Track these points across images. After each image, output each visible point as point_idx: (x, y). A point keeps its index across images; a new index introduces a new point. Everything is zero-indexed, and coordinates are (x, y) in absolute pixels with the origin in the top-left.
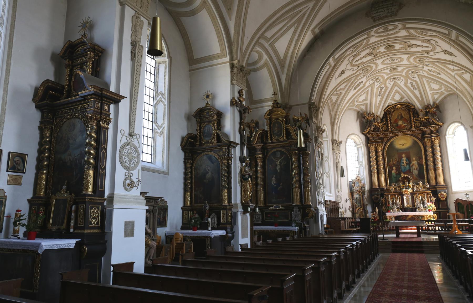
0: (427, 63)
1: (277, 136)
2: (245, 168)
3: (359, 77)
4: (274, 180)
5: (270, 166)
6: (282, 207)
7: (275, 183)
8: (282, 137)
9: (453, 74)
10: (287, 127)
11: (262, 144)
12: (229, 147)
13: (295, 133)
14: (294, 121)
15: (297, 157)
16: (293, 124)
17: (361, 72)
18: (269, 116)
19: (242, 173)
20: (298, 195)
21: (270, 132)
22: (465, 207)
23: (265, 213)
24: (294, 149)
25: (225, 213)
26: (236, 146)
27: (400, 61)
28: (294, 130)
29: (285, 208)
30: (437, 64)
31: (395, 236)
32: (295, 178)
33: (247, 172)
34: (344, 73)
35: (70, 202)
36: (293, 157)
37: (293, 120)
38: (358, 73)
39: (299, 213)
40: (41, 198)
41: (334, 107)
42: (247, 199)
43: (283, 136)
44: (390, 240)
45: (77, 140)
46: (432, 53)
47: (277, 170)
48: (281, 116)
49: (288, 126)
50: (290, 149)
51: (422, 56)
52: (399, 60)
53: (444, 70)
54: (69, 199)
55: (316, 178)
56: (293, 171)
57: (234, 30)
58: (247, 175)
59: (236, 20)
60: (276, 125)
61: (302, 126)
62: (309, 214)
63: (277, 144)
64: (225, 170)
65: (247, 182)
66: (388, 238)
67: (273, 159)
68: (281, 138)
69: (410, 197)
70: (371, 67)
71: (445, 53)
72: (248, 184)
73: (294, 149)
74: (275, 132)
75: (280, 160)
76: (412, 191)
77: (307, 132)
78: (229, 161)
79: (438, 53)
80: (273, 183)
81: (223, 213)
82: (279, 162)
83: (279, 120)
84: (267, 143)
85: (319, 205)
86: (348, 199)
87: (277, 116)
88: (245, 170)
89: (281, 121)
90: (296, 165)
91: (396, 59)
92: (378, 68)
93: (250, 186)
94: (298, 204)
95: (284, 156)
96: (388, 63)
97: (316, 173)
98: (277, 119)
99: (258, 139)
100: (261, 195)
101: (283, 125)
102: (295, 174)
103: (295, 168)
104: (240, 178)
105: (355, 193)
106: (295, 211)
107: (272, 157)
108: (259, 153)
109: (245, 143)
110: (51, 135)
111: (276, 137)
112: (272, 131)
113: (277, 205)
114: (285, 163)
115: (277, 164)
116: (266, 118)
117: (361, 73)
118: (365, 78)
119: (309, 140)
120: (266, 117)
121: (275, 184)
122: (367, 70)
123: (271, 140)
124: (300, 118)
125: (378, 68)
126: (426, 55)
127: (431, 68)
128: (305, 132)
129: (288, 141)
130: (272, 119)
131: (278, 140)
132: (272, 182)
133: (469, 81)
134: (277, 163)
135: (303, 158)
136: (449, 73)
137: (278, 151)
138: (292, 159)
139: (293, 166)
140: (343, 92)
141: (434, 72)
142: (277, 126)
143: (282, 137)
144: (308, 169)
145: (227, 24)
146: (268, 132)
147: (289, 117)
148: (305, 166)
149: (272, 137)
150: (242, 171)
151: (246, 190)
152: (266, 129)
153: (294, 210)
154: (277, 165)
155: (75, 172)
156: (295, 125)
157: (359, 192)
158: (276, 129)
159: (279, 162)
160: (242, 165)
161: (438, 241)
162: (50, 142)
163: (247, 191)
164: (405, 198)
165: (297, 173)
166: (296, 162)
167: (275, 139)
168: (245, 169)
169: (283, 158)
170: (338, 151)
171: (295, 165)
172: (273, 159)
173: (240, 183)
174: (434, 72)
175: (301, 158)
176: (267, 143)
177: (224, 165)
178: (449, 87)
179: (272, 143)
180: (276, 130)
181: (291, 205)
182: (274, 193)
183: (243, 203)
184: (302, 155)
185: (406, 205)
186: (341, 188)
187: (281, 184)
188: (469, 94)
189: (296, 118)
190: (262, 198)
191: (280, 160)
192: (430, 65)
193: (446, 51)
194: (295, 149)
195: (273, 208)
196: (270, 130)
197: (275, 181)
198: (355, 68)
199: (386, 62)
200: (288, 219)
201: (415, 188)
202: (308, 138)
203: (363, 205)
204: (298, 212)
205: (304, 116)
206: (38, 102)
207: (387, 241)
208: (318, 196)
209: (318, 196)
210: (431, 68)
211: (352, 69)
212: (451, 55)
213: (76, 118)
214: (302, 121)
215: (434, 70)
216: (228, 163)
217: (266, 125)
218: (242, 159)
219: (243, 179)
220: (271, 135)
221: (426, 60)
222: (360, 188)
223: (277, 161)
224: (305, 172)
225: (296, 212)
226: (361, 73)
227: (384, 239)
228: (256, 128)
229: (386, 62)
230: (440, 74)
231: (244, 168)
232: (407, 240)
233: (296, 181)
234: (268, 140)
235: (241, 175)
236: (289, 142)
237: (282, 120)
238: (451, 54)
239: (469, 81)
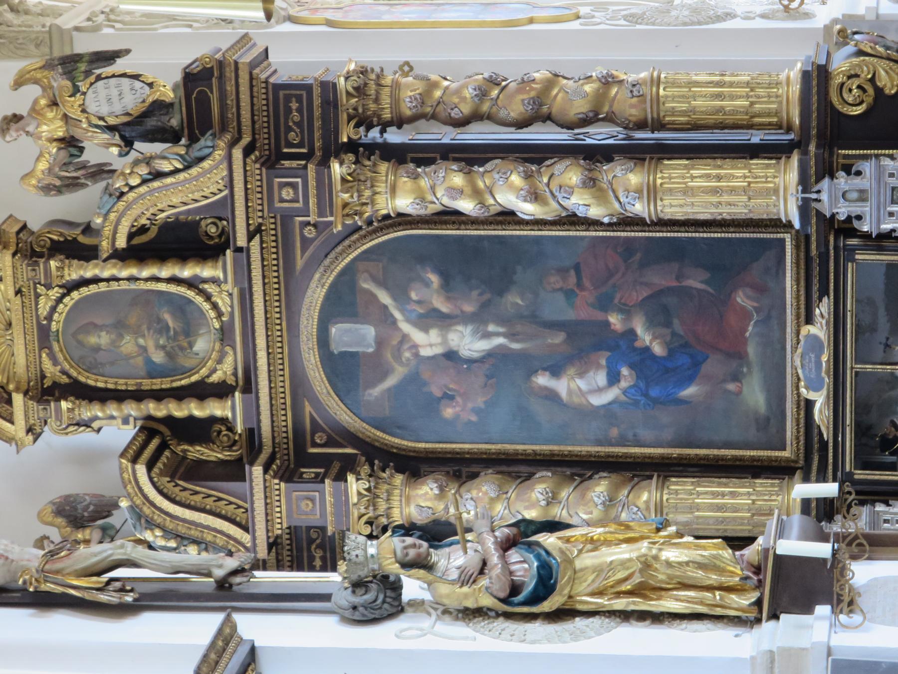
1: (191, 345)
2: (442, 579)
4: (582, 384)
5: (448, 412)
6: (809, 320)
7: (601, 378)
8: (208, 297)
10: (121, 243)
11: (257, 471)
13: (176, 171)
14: (72, 185)
15: (383, 167)
16: (95, 190)
18: (9, 402)
19: (487, 601)
20: (719, 178)
21: (159, 396)
23: (860, 475)
24: (312, 192)
26: (243, 652)
28: (144, 182)
29: (824, 292)
32: (571, 191)
36: (386, 205)
37: (59, 190)
39: (867, 167)
42: (720, 570)
43: (190, 283)
47: (490, 355)
48: (18, 292)
49: (107, 231)
50: (310, 233)
55: (575, 25)
56: (507, 217)
60: (93, 340)
61: (118, 108)
62: (879, 91)
63: (261, 342)
65: (570, 562)
67: (391, 382)
68: (215, 306)
72: (586, 561)
73: (312, 192)
74: (158, 357)
75: (406, 327)
77: (178, 77)
80: (600, 390)
82: (418, 336)
83: (49, 318)
84: (252, 434)
85: (807, 16)
87: (17, 329)
88: (467, 579)
89: (59, 300)
90: (458, 180)
93: (608, 543)
94: (792, 176)
95: (365, 286)
97: (531, 21)
98: (44, 335)
99: (209, 503)
100: (698, 508)
101: (96, 280)
102: (535, 196)
103: (477, 194)
104: (537, 628)
106: (855, 209)
107: (376, 391)
108: (336, 505)
109: (219, 573)
111: (201, 345)
112: (147, 384)
113: (794, 360)
114: (434, 279)
115: (439, 350)
116: (30, 430)
119: (247, 59)
120: (18, 429)
121: (614, 379)
123: (222, 391)
124: (53, 127)
128: (175, 89)
129: (241, 241)
130: (43, 377)
131: (225, 334)
132: (598, 400)
134: (425, 352)
135: (400, 122)
137: (323, 341)
138: (402, 220)
139: (467, 206)
142: (103, 339)
143: (208, 297)
144: (493, 81)
146: (150, 418)
147: (35, 225)
148: (466, 109)
149: (201, 383)
150: (470, 604)
151: (637, 579)
152: (127, 433)
153: (843, 211)
154: (451, 356)
156: (101, 171)
158: (128, 345)
159: (418, 336)
160: (417, 605)
163: (647, 565)
165: (528, 176)
166: (424, 183)
167: (220, 361)
168: (454, 575)
169: (384, 298)
171: (458, 192)
172: (391, 382)
173: (579, 622)
175: (394, 136)
176: (252, 434)
179: (249, 386)
180: (144, 349)
181: (802, 240)
182: (690, 391)
183: (759, 603)
184: (375, 134)
187: (615, 320)
189: (43, 166)
190: (733, 495)
191: (406, 327)
194: (312, 183)
195: (820, 400)
196: (138, 396)
197: (581, 374)
202: (221, 64)
204: (857, 182)
205: (32, 91)
208: (730, 16)
209: (730, 16)
214: (75, 113)
217: (85, 437)
218: (357, 600)
219: (544, 598)
220: (180, 394)
223: (415, 346)
224: (516, 109)
225: (863, 196)
228: (115, 520)
231: (444, 589)
233: (590, 183)
234: (223, 421)
235: (508, 616)
237: (55, 293)
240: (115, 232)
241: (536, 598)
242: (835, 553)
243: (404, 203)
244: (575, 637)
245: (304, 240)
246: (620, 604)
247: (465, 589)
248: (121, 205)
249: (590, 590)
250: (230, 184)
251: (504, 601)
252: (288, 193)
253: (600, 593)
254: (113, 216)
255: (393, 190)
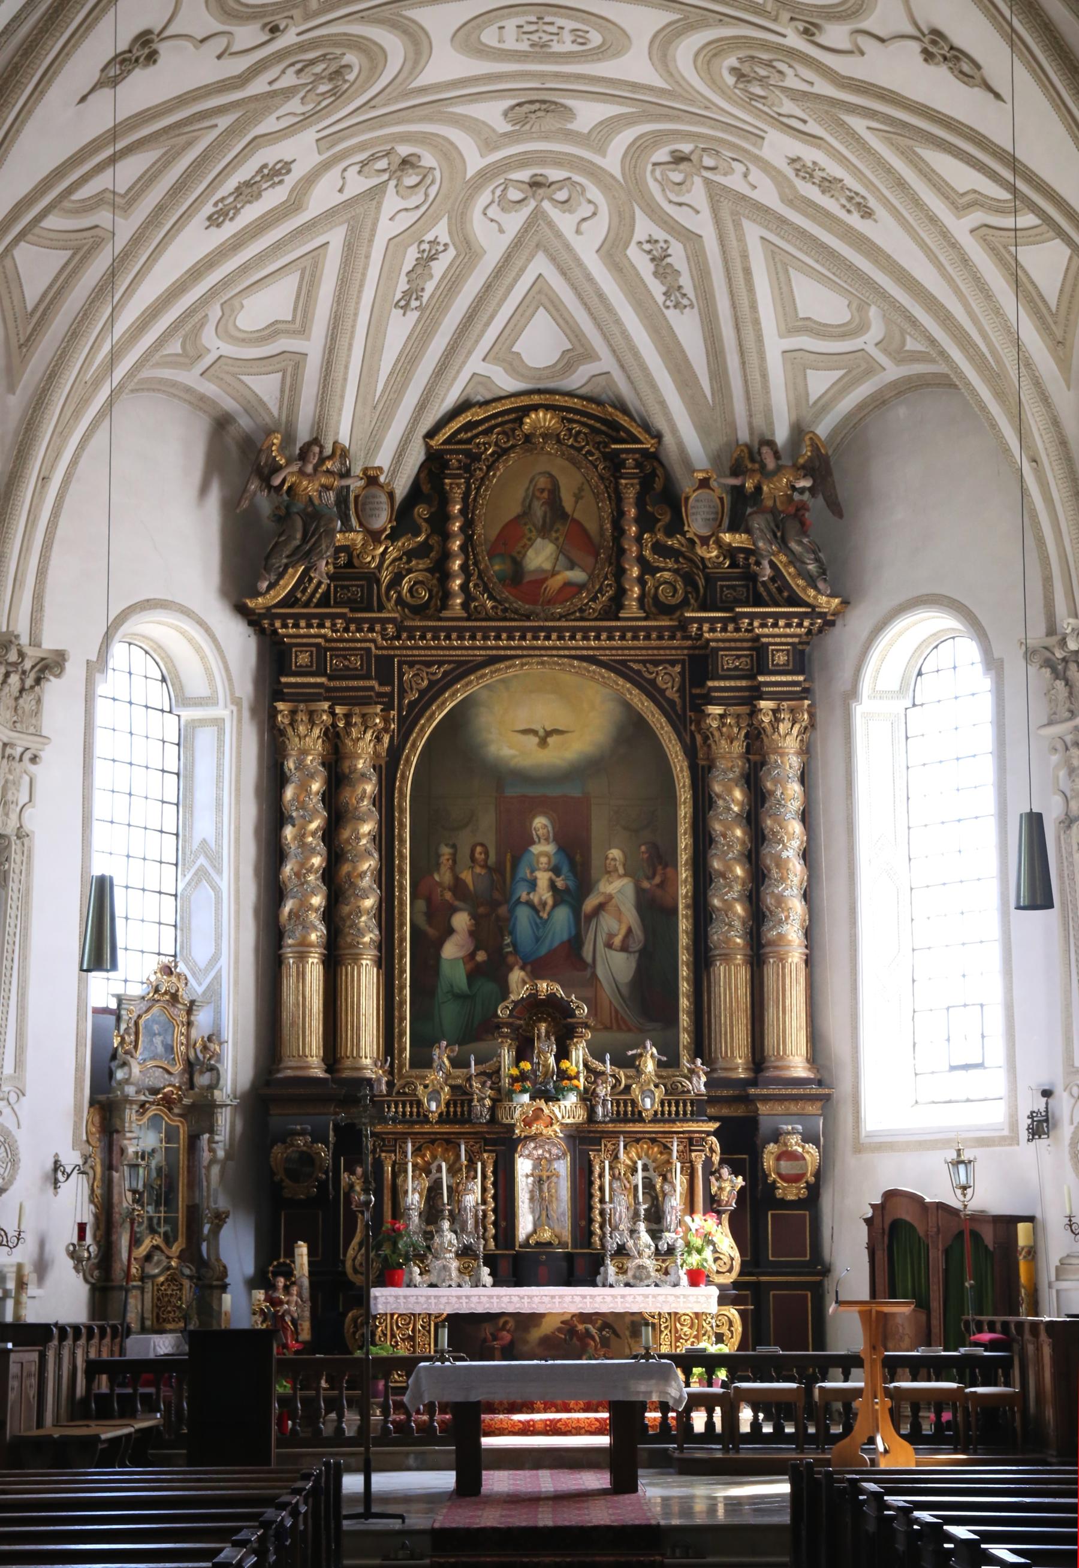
0: (788, 107)
3: (269, 124)
9: (960, 227)
17: (289, 79)
22: (936, 1256)
27: (600, 53)
30: (858, 124)
31: (446, 1480)
34: (152, 58)
38: (258, 86)
41: (28, 343)
44: (417, 1521)
46: (836, 34)
51: (765, 45)
52: (595, 38)
53: (901, 184)
66: (407, 1499)
69: (563, 1167)
70: (374, 54)
71: (928, 56)
76: (581, 1115)
79: (882, 40)
86: (71, 1158)
91: (569, 24)
92: (433, 73)
96: (511, 44)
105: (130, 1114)
117: (288, 93)
118: (310, 135)
122: (338, 74)
125: (433, 73)
126: (794, 40)
127: (810, 154)
133: (1053, 302)
136: (933, 220)
140: (126, 228)
141: (828, 185)
157: (168, 1102)
161: (786, 1519)
164: (523, 1166)
170: (21, 742)
174: (828, 185)
178: (914, 322)
185: (525, 1224)
186: (19, 1063)
188: (1045, 399)
192: (813, 127)
193: (937, 34)
198: (248, 34)
199: (489, 37)
201: (603, 1091)
203: (194, 1213)
207: (395, 1524)
210: (810, 154)
211: (218, 45)
212: (965, 77)
215: (835, 170)
221: (791, 82)
222: (177, 1069)
226: (288, 93)
227: (368, 1514)
229: (489, 37)
230: (867, 213)
232: (545, 1518)
238: (966, 67)
239: (1053, 302)
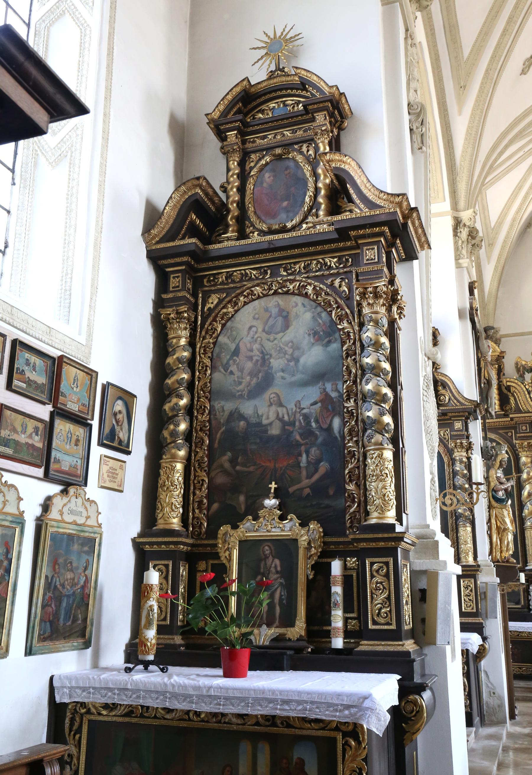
12: (469, 418)
19: (492, 485)
25: (472, 586)
28: (527, 389)
33: (501, 483)
35: (309, 547)
40: (171, 533)
45: (302, 360)
54: (303, 541)
57: (466, 139)
58: (502, 490)
59: (473, 115)
64: (464, 476)
78: (469, 452)
81: (466, 588)
110: (192, 344)
145: (449, 123)
150: (491, 479)
155: (304, 456)
162: (191, 363)
177: (461, 462)
183: (498, 561)
200: (518, 603)
206: (158, 243)
213: (293, 294)
216: (469, 458)
236: (511, 418)
240: (511, 382)
241: (494, 498)
242: (523, 584)
243: (523, 459)
244: (485, 510)
245: (507, 433)
246: (493, 521)
247: (495, 478)
248: (520, 384)
249: (497, 513)
250: (526, 413)
251: (493, 489)
252: (524, 428)
253: (496, 516)
254: (516, 381)
255: (527, 456)
